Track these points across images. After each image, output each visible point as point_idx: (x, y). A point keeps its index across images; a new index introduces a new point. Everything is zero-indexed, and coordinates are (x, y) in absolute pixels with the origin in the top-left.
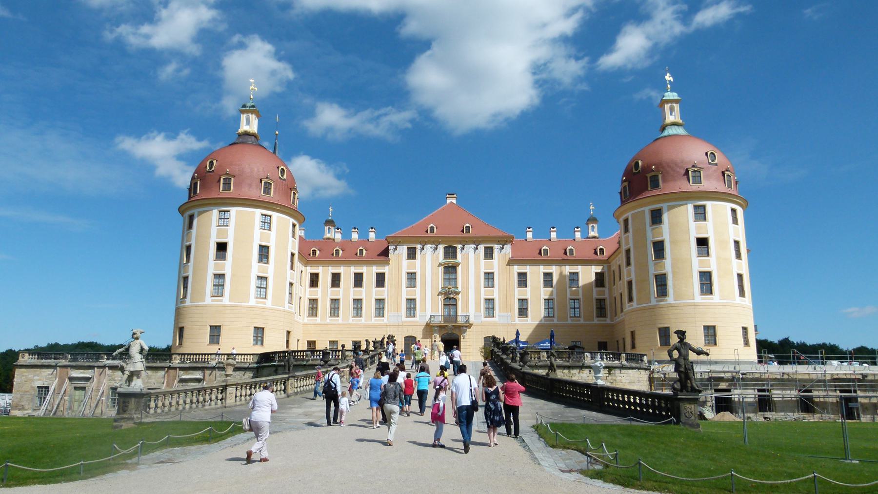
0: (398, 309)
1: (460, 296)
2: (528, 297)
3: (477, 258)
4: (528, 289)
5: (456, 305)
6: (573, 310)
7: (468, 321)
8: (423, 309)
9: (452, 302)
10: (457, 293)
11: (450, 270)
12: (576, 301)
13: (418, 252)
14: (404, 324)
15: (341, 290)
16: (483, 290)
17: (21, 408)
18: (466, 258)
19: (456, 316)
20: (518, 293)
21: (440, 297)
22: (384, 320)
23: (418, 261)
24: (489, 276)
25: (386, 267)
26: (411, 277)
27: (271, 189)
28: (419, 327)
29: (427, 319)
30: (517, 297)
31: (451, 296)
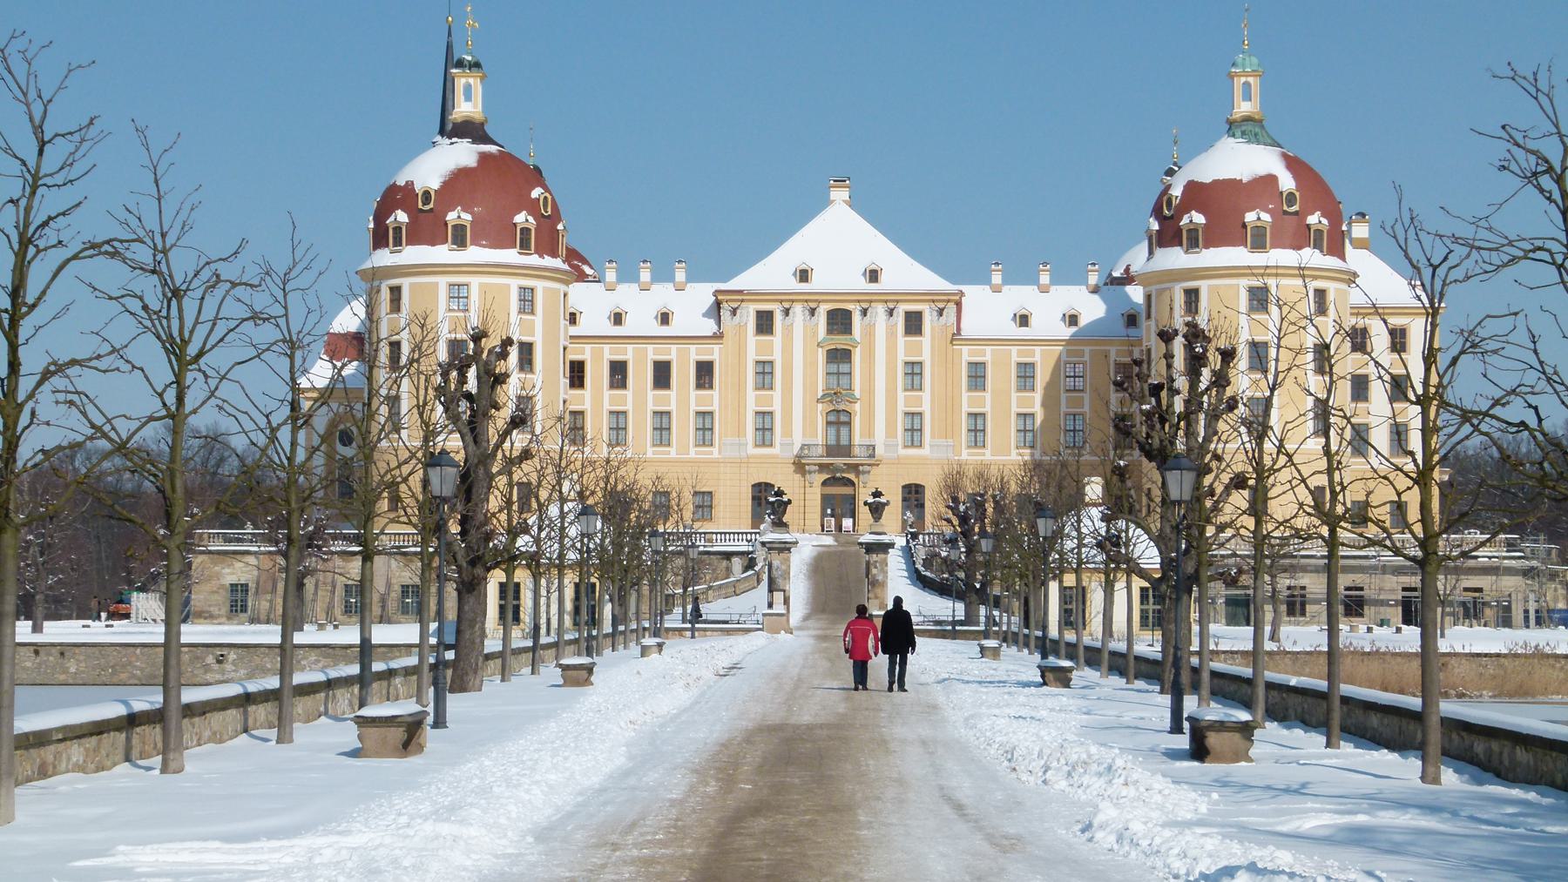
0: (740, 432)
1: (857, 407)
2: (987, 409)
3: (891, 335)
4: (988, 395)
5: (849, 424)
6: (1072, 434)
7: (872, 456)
8: (788, 432)
9: (843, 418)
10: (853, 401)
11: (839, 356)
12: (1077, 417)
13: (778, 317)
14: (751, 460)
15: (628, 394)
16: (901, 395)
17: (207, 615)
18: (870, 332)
19: (850, 446)
20: (967, 402)
21: (820, 406)
22: (714, 453)
23: (777, 338)
24: (914, 371)
25: (716, 347)
26: (765, 371)
27: (530, 239)
28: (780, 465)
29: (796, 450)
30: (965, 409)
31: (841, 407)
